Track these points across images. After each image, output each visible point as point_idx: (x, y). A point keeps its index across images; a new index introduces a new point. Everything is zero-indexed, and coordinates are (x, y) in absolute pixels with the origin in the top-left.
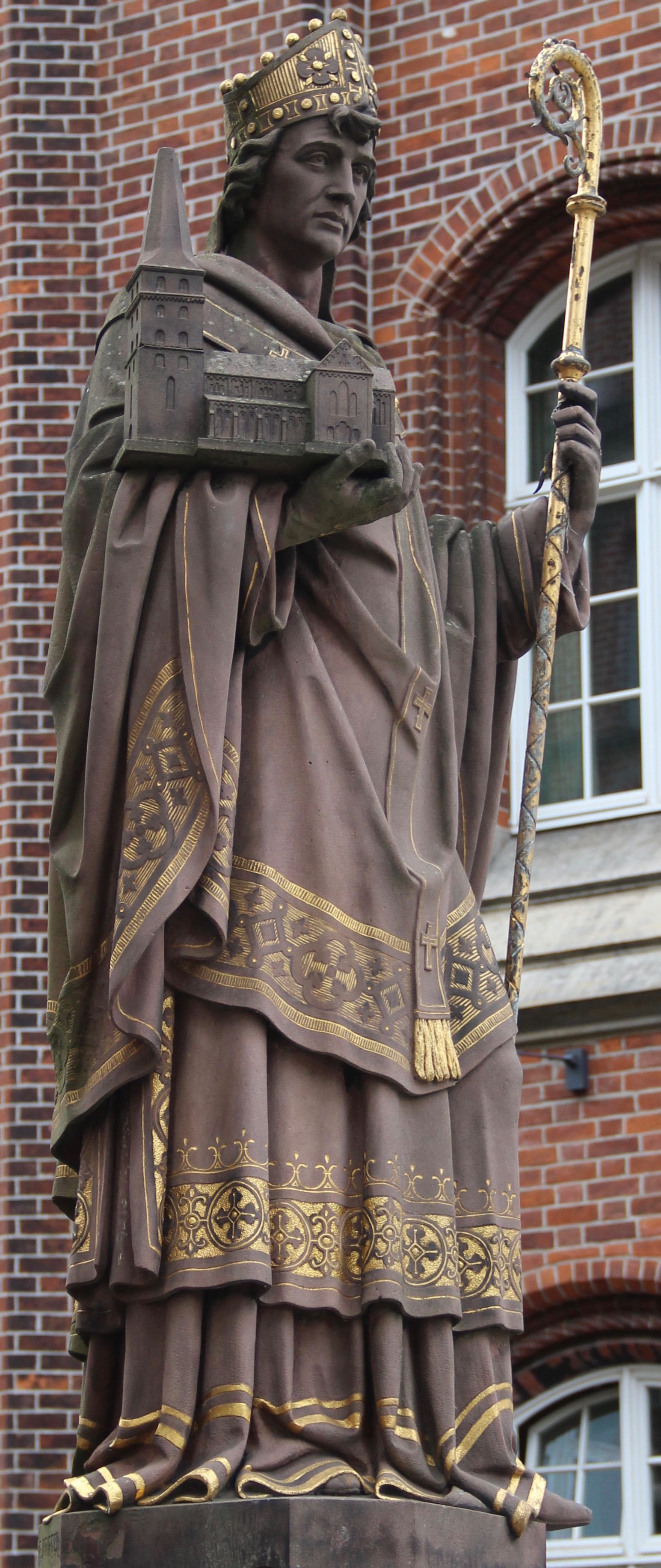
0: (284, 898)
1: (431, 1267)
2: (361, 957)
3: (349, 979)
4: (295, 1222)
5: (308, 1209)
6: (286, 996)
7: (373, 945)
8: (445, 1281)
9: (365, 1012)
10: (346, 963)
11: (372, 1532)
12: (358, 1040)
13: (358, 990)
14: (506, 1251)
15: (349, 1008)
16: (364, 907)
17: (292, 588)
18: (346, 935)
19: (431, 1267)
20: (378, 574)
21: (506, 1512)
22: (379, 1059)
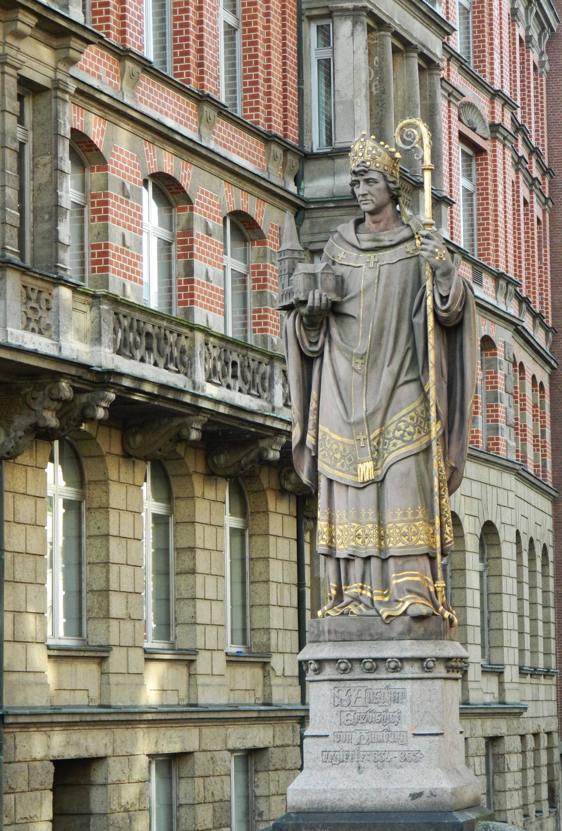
0: (325, 434)
1: (366, 540)
2: (341, 448)
3: (338, 456)
4: (338, 532)
5: (341, 527)
6: (327, 464)
7: (344, 443)
8: (370, 545)
9: (342, 465)
10: (337, 451)
11: (321, 629)
12: (341, 474)
13: (341, 459)
14: (397, 531)
15: (339, 464)
16: (340, 433)
17: (322, 336)
18: (337, 442)
19: (366, 540)
20: (351, 320)
21: (380, 615)
22: (345, 479)
